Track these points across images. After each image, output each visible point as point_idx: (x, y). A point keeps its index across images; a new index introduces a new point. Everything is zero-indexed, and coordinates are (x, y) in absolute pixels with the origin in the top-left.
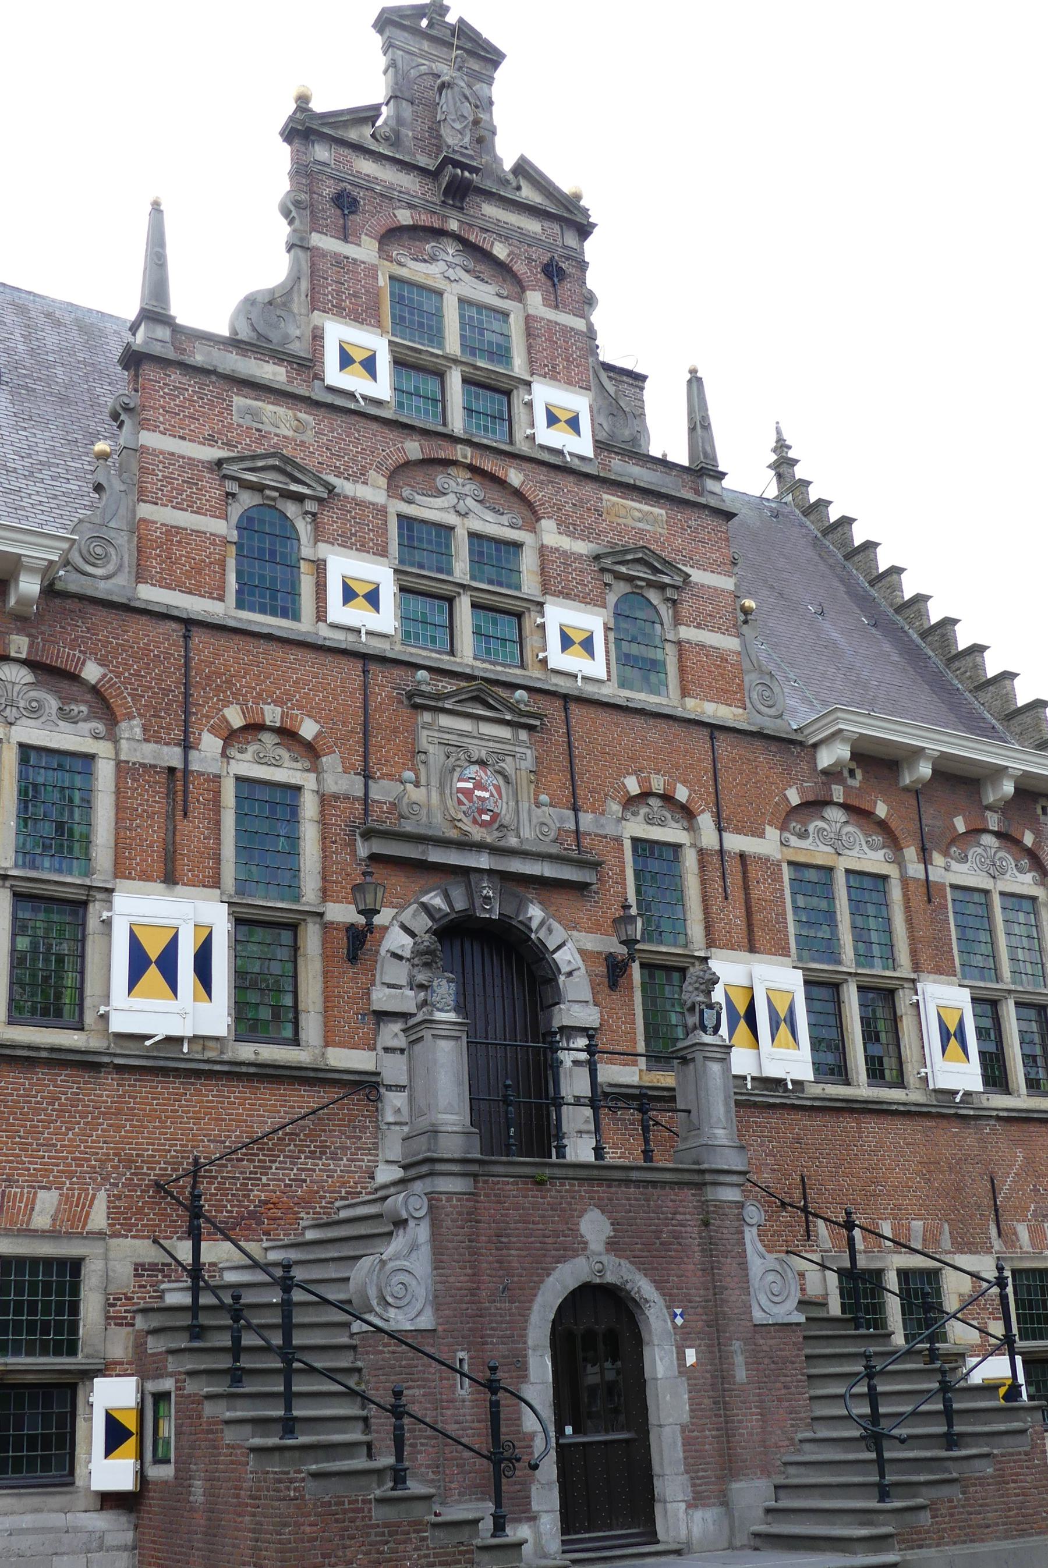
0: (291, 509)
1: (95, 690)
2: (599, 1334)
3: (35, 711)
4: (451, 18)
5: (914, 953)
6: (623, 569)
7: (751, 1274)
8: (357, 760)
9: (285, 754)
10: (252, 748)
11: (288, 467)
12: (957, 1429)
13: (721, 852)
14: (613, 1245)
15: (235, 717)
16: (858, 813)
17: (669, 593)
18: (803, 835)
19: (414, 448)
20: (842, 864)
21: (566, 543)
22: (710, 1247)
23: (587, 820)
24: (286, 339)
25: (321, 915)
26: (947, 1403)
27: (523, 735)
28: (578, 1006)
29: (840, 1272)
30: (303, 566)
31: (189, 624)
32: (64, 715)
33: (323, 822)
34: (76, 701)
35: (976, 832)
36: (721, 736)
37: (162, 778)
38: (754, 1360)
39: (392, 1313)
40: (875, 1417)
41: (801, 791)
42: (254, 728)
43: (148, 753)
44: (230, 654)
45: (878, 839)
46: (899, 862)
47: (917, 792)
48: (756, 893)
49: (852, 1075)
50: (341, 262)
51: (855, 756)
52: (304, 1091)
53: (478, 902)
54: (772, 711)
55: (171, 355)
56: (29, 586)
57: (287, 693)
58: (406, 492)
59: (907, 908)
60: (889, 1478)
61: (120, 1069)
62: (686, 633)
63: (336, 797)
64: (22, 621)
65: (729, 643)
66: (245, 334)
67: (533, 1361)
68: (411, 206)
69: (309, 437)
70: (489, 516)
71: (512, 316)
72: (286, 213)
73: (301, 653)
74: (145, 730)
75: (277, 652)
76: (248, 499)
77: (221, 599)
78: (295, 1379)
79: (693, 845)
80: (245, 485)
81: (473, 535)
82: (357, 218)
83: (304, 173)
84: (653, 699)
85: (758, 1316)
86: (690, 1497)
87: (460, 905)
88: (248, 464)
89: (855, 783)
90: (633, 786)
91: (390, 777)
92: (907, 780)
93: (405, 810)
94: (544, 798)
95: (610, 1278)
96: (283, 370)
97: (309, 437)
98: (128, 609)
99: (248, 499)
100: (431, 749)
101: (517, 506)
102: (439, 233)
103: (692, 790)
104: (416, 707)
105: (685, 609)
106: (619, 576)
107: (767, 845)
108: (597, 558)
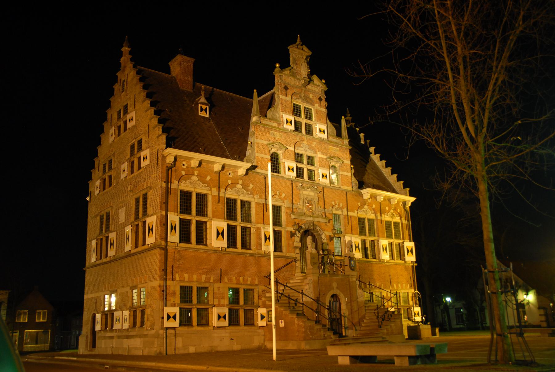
13: (348, 215)
14: (337, 288)
21: (322, 156)
50: (286, 101)
81: (308, 156)
82: (288, 91)
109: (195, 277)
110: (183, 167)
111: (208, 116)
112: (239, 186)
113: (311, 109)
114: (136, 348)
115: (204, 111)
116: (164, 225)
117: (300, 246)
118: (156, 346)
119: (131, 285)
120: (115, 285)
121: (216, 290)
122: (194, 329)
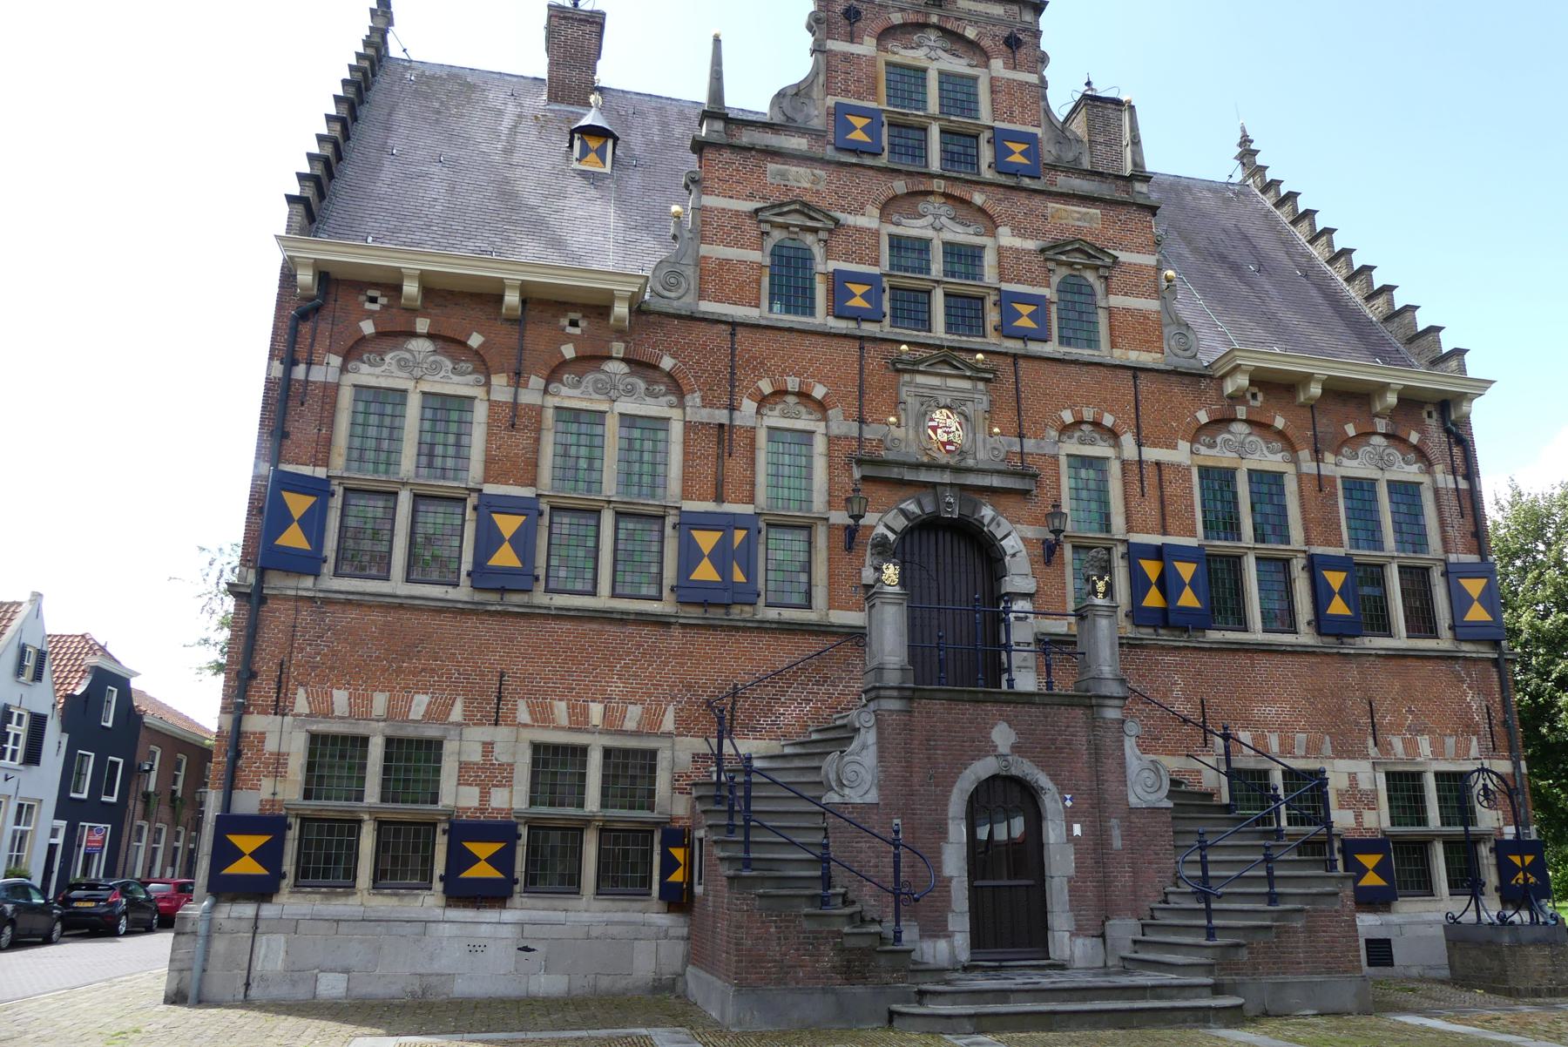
0: (809, 239)
1: (669, 374)
3: (630, 392)
5: (1306, 530)
6: (1064, 258)
7: (1129, 772)
8: (854, 411)
9: (803, 410)
10: (779, 407)
11: (806, 209)
12: (1277, 890)
13: (1140, 462)
14: (1016, 749)
15: (766, 387)
16: (1259, 425)
17: (1101, 272)
18: (1212, 446)
19: (900, 186)
20: (1245, 466)
21: (1018, 243)
22: (1097, 752)
23: (1030, 444)
24: (808, 117)
25: (827, 519)
26: (1270, 871)
27: (981, 385)
28: (1019, 577)
30: (818, 278)
31: (734, 325)
33: (829, 456)
34: (656, 383)
35: (1365, 435)
36: (1142, 376)
37: (715, 432)
38: (1128, 834)
39: (847, 791)
40: (1205, 879)
41: (1209, 413)
42: (781, 393)
43: (705, 415)
44: (760, 345)
45: (1277, 445)
46: (1295, 461)
47: (1312, 407)
48: (1168, 491)
49: (1250, 624)
50: (847, 58)
51: (1252, 382)
53: (942, 506)
54: (1188, 353)
55: (723, 141)
56: (621, 309)
57: (804, 367)
58: (895, 218)
59: (1301, 496)
60: (1215, 922)
61: (684, 626)
62: (1116, 301)
63: (838, 438)
65: (1153, 305)
67: (952, 827)
68: (902, 10)
70: (959, 229)
71: (980, 81)
72: (810, 28)
73: (813, 339)
74: (703, 399)
75: (795, 338)
76: (777, 235)
77: (757, 306)
78: (752, 832)
79: (1118, 458)
80: (774, 225)
82: (861, 24)
84: (1087, 352)
85: (1133, 801)
86: (1073, 928)
87: (929, 509)
88: (777, 210)
89: (1257, 403)
90: (1068, 417)
91: (879, 421)
92: (1302, 398)
93: (889, 444)
94: (996, 430)
95: (1014, 772)
96: (804, 141)
97: (821, 186)
98: (693, 318)
99: (777, 235)
100: (909, 400)
101: (981, 218)
102: (923, 26)
103: (1117, 417)
104: (898, 371)
105: (1114, 282)
106: (1060, 263)
107: (1181, 454)
108: (1042, 251)
109: (380, 702)
110: (368, 306)
111: (608, 169)
112: (616, 368)
113: (975, 79)
115: (592, 157)
121: (476, 756)
122: (354, 901)
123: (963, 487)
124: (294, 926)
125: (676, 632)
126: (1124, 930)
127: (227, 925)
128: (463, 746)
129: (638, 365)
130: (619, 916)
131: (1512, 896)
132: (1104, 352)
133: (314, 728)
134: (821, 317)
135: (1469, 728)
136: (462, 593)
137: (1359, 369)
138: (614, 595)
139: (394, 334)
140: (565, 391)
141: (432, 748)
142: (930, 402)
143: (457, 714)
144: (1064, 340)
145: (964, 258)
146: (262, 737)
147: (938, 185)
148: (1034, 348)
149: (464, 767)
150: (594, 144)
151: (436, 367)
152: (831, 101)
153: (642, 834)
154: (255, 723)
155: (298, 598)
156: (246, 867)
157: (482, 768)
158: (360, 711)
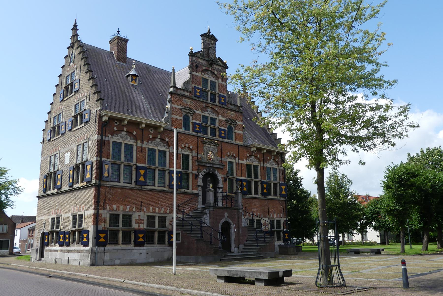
0: (189, 115)
1: (167, 142)
2: (226, 227)
3: (160, 145)
4: (211, 34)
8: (197, 151)
11: (190, 109)
14: (228, 217)
16: (256, 157)
18: (248, 160)
19: (204, 105)
20: (253, 164)
24: (189, 88)
29: (250, 220)
32: (164, 146)
35: (270, 159)
46: (260, 164)
48: (243, 169)
50: (196, 76)
52: (190, 196)
62: (237, 131)
64: (160, 133)
65: (241, 132)
66: (184, 88)
69: (192, 104)
72: (189, 68)
80: (184, 112)
82: (198, 69)
83: (192, 62)
87: (208, 171)
90: (228, 154)
97: (192, 104)
99: (184, 114)
102: (208, 70)
107: (244, 162)
109: (121, 207)
110: (115, 124)
111: (137, 84)
112: (158, 140)
113: (216, 82)
114: (75, 260)
115: (134, 81)
116: (99, 168)
117: (202, 185)
118: (89, 259)
119: (72, 212)
120: (60, 211)
121: (138, 218)
122: (119, 246)
123: (213, 167)
124: (110, 251)
125: (169, 194)
126: (241, 246)
127: (100, 251)
128: (135, 217)
129: (162, 140)
130: (162, 247)
131: (285, 240)
132: (233, 141)
133: (111, 213)
134: (191, 132)
135: (281, 212)
136: (133, 185)
137: (271, 148)
138: (158, 186)
139: (120, 130)
140: (149, 144)
141: (130, 216)
142: (208, 150)
143: (134, 210)
144: (228, 139)
145: (213, 120)
146: (101, 215)
147: (210, 105)
148: (224, 140)
149: (136, 220)
150: (134, 78)
151: (127, 138)
152: (193, 85)
153: (164, 233)
154: (101, 212)
155: (107, 186)
156: (102, 240)
157: (138, 220)
158: (118, 210)
